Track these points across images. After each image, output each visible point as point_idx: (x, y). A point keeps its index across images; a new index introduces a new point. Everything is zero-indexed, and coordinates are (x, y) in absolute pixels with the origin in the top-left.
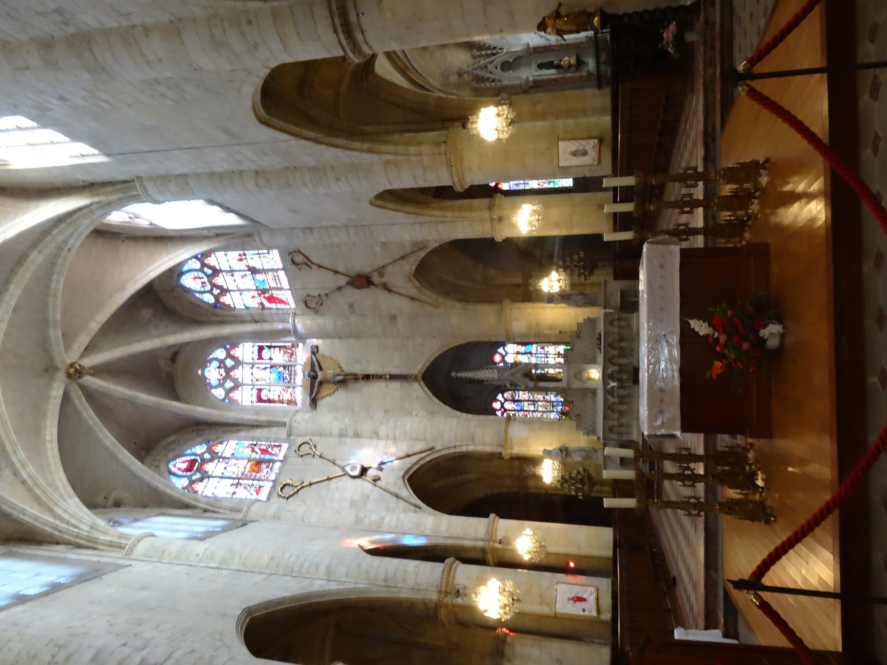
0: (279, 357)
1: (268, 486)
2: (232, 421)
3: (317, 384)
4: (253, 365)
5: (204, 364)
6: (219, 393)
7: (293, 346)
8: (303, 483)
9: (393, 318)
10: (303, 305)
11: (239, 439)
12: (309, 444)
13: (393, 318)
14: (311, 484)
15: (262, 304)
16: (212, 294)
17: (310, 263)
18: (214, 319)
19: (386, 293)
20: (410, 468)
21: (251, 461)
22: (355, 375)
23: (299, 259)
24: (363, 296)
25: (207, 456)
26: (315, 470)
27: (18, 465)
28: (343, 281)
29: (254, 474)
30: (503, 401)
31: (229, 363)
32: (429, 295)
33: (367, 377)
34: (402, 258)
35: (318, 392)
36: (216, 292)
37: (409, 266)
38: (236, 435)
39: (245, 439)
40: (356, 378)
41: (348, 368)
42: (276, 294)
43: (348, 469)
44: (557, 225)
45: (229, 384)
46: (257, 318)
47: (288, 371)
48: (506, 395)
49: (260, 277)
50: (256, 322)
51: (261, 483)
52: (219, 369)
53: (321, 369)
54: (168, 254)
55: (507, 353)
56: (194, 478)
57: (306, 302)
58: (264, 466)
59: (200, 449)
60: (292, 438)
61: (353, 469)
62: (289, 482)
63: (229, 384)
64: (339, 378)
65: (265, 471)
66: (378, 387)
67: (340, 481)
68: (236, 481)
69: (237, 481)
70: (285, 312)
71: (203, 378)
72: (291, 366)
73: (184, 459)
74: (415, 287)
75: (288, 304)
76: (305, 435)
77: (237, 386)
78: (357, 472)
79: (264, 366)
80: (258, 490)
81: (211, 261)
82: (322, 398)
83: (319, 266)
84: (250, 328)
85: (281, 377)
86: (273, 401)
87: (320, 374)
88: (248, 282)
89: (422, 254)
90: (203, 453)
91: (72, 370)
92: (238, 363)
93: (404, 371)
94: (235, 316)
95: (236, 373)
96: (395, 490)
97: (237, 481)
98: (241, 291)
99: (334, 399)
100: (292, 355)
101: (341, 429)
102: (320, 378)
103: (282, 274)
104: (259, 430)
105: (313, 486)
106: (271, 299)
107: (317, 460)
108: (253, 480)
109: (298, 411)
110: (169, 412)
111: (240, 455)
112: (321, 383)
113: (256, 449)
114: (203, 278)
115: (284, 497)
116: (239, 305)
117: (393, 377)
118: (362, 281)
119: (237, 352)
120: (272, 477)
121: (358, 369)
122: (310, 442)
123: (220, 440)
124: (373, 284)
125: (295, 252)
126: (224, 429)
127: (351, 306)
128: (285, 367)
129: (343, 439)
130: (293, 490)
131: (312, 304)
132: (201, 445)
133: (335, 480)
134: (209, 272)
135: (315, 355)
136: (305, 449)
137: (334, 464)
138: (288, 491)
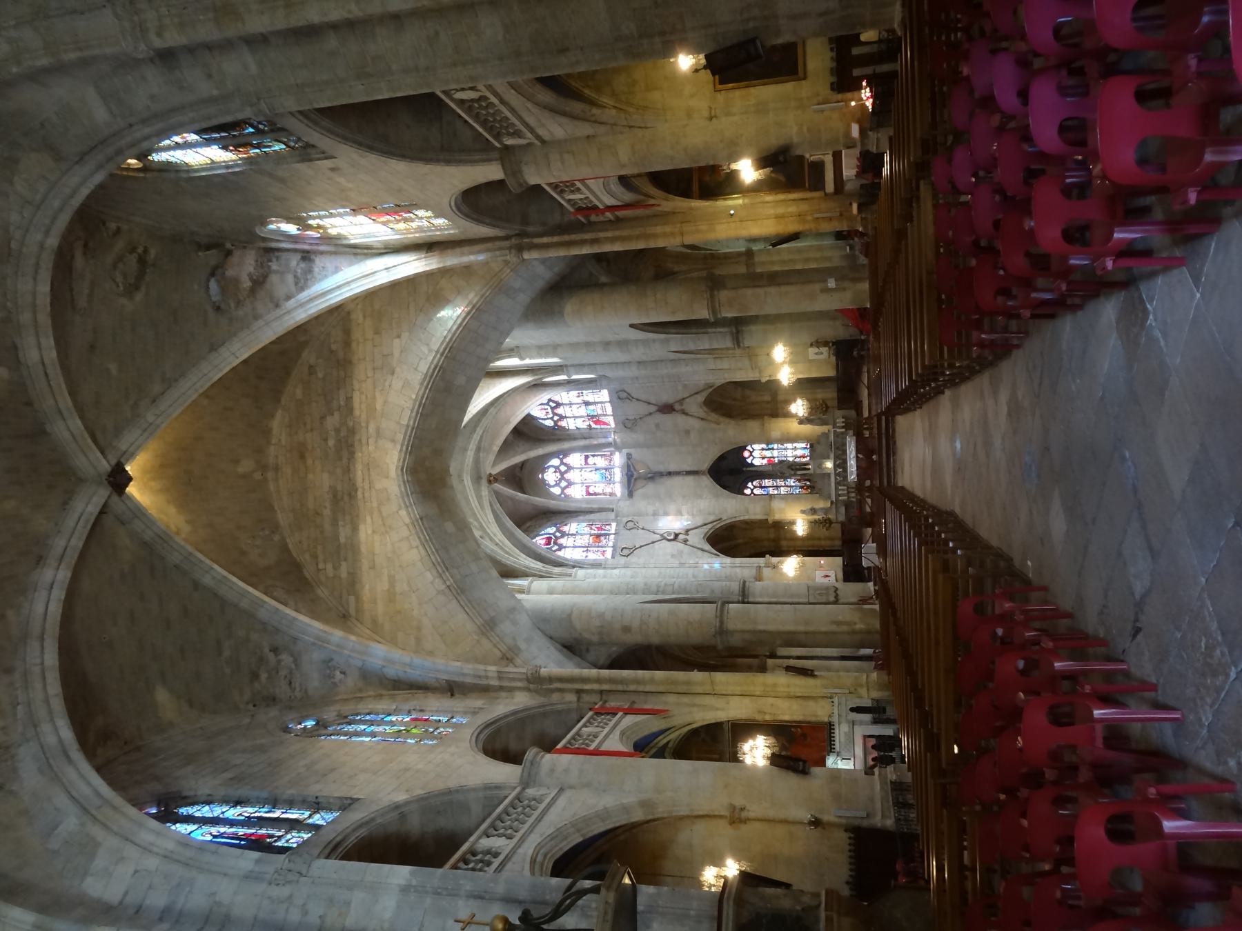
3: (633, 480)
4: (581, 469)
5: (543, 471)
6: (556, 491)
9: (687, 432)
10: (622, 426)
11: (579, 522)
13: (687, 432)
15: (590, 426)
18: (553, 437)
20: (708, 532)
22: (662, 473)
23: (624, 395)
24: (667, 420)
26: (641, 537)
27: (492, 535)
28: (653, 409)
29: (597, 544)
30: (752, 487)
32: (714, 416)
33: (670, 474)
34: (697, 393)
35: (634, 485)
37: (701, 398)
38: (576, 519)
39: (583, 521)
42: (603, 419)
43: (665, 535)
44: (801, 373)
45: (564, 484)
48: (754, 483)
49: (591, 407)
50: (585, 438)
51: (604, 549)
53: (635, 470)
54: (535, 397)
55: (754, 450)
58: (602, 538)
59: (551, 530)
62: (625, 546)
63: (564, 484)
64: (649, 475)
65: (604, 541)
66: (677, 480)
68: (585, 549)
69: (587, 548)
71: (543, 480)
74: (705, 412)
75: (610, 425)
77: (570, 484)
78: (672, 537)
79: (590, 469)
81: (557, 398)
82: (637, 489)
83: (638, 400)
84: (582, 443)
85: (603, 476)
86: (600, 494)
87: (635, 473)
88: (583, 411)
89: (711, 390)
90: (555, 532)
91: (492, 478)
92: (569, 468)
93: (695, 469)
94: (569, 435)
96: (700, 546)
97: (587, 548)
98: (575, 417)
99: (643, 490)
100: (611, 460)
102: (635, 477)
106: (597, 422)
107: (641, 531)
109: (619, 500)
110: (533, 505)
111: (583, 532)
112: (636, 479)
113: (593, 527)
116: (572, 427)
118: (667, 409)
120: (611, 544)
121: (661, 468)
124: (674, 410)
125: (621, 391)
126: (567, 515)
127: (657, 426)
128: (606, 469)
129: (656, 517)
134: (553, 405)
136: (630, 525)
138: (626, 552)
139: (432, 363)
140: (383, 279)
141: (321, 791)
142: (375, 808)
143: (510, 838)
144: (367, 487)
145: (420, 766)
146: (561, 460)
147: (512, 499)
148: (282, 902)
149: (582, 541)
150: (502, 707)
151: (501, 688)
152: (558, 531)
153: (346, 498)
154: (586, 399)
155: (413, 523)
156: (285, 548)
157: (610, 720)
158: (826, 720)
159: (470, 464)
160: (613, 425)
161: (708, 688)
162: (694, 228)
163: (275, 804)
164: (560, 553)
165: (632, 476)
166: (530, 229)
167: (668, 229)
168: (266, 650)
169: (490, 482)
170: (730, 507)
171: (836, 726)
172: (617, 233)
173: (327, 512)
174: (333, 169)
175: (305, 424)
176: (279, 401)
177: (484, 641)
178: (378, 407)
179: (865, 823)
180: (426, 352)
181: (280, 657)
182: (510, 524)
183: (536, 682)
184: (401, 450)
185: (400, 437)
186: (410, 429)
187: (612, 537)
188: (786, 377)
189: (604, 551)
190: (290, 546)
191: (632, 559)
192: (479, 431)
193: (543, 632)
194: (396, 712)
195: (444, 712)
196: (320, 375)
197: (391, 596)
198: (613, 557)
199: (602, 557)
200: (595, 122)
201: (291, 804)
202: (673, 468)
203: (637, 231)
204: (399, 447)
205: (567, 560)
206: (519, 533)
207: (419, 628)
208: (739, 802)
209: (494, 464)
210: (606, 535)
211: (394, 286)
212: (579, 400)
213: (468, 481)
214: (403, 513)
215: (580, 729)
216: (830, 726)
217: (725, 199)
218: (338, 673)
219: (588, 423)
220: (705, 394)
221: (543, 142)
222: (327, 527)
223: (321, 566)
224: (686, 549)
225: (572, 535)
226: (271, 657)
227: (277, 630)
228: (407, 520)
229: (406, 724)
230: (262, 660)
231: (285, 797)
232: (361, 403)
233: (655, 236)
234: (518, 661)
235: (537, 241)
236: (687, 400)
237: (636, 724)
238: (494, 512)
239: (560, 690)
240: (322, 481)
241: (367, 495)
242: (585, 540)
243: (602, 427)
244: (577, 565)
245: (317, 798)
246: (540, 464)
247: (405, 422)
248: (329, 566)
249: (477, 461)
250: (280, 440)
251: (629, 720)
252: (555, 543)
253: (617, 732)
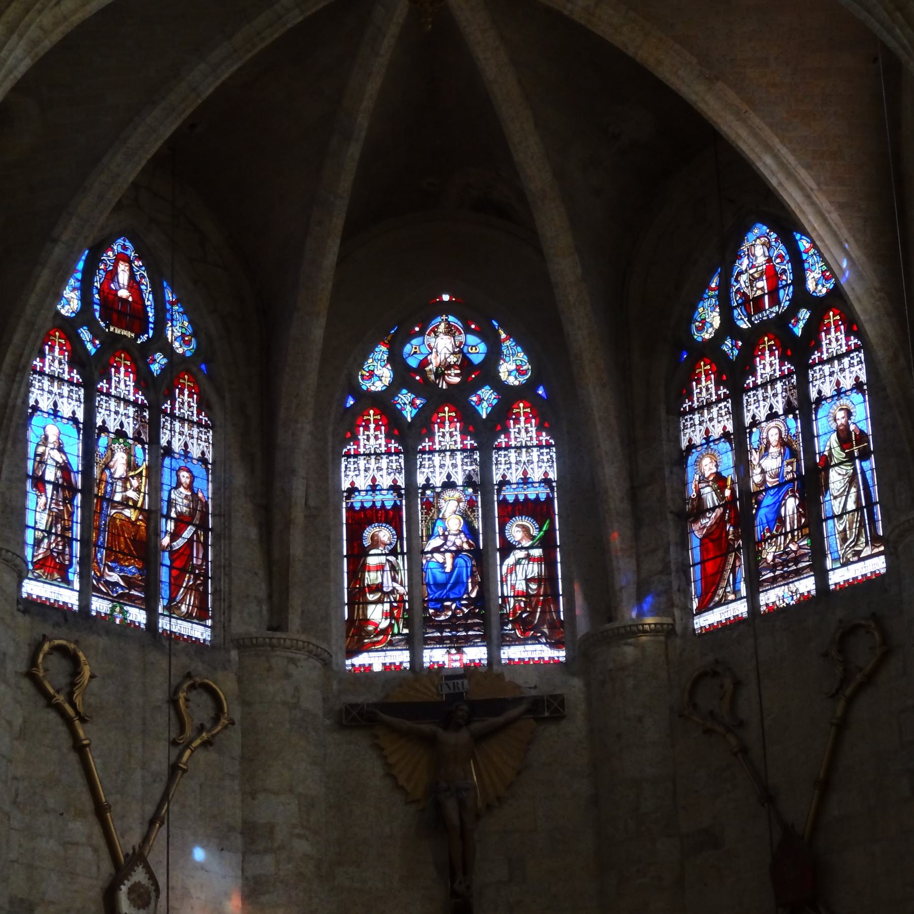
3: (426, 727)
7: (555, 626)
8: (83, 720)
12: (216, 720)
14: (80, 749)
15: (700, 510)
16: (720, 335)
17: (848, 691)
21: (147, 520)
25: (157, 366)
29: (104, 538)
43: (139, 876)
47: (466, 617)
50: (633, 495)
52: (460, 367)
53: (479, 738)
54: (840, 207)
56: (85, 334)
57: (715, 674)
60: (234, 654)
62: (87, 671)
64: (451, 807)
67: (96, 850)
68: (78, 480)
70: (677, 598)
72: (485, 625)
73: (146, 287)
76: (245, 703)
79: (479, 525)
82: (378, 748)
83: (842, 726)
87: (463, 736)
90: (168, 351)
101: (271, 829)
103: (807, 585)
104: (253, 533)
105: (73, 757)
107: (161, 757)
108: (85, 542)
109: (326, 663)
111: (167, 478)
113: (188, 533)
114: (775, 301)
115: (33, 662)
122: (224, 721)
123: (214, 398)
128: (482, 601)
129: (238, 841)
130: (58, 691)
132: (194, 334)
133: (97, 830)
135: (528, 711)
137: (152, 823)
146: (524, 392)
154: (837, 478)
160: (704, 621)
165: (448, 721)
189: (63, 571)
219: (710, 497)
225: (155, 429)
243: (695, 573)
252: (111, 345)
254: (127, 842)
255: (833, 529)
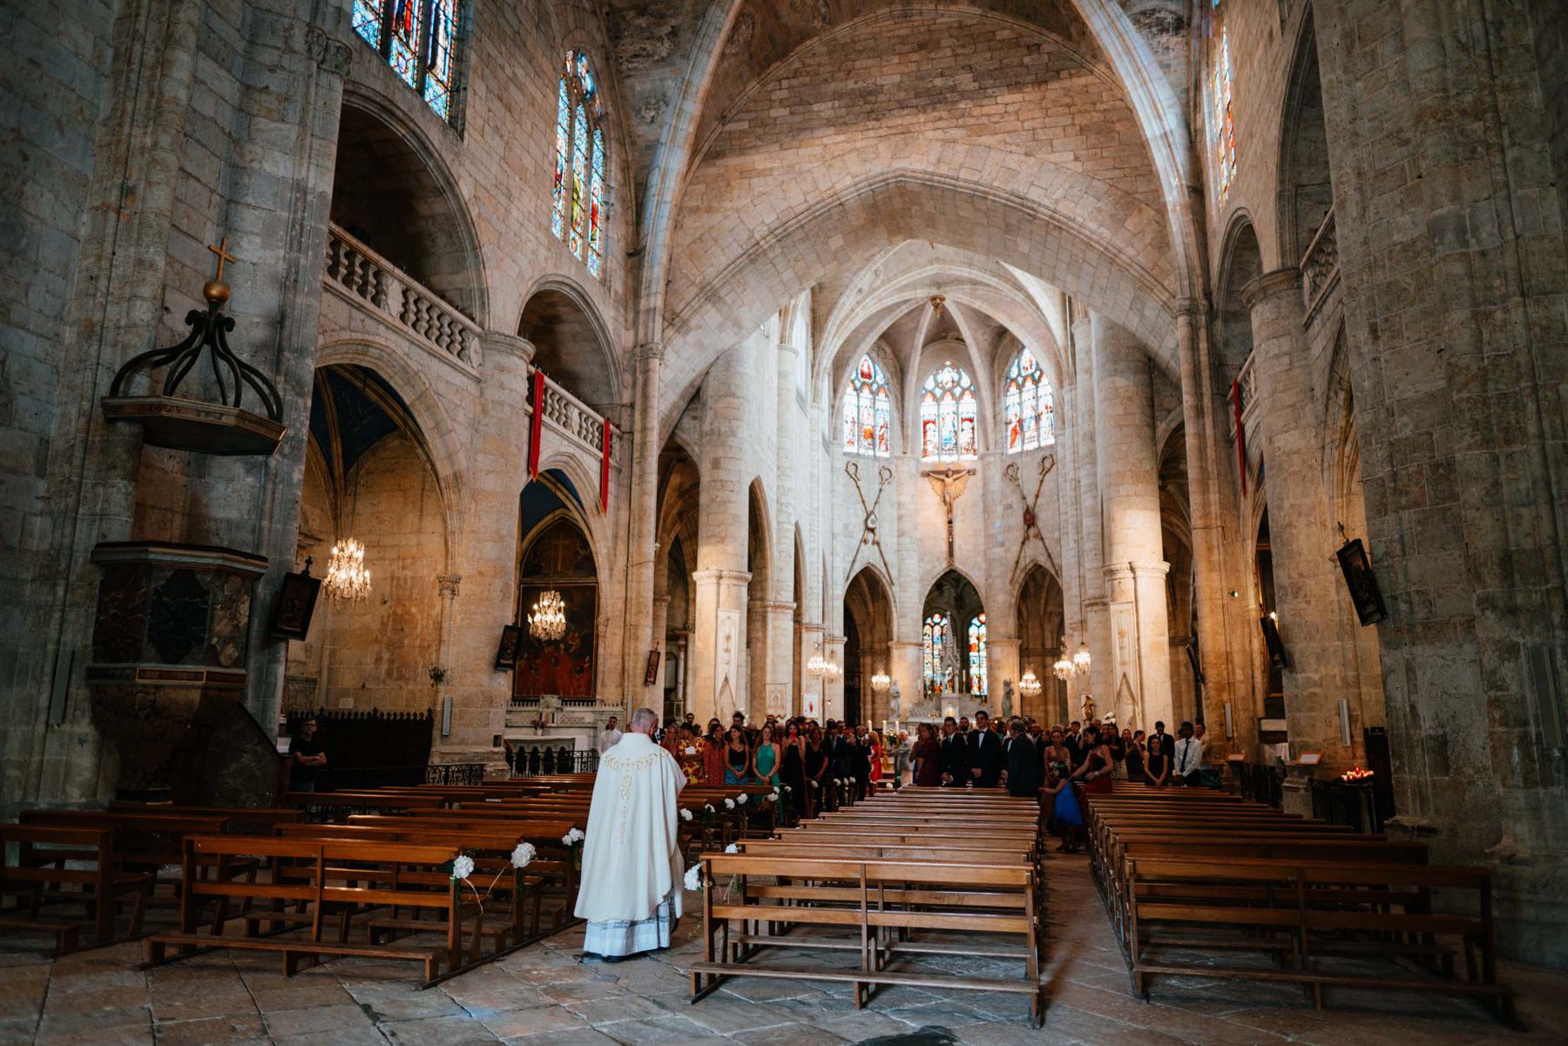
0: (965, 438)
1: (854, 449)
2: (906, 405)
6: (930, 384)
19: (1021, 540)
23: (1048, 464)
24: (1018, 519)
28: (1030, 501)
31: (958, 391)
32: (1020, 576)
34: (1049, 556)
36: (1020, 380)
37: (1043, 560)
39: (891, 418)
40: (950, 511)
41: (955, 504)
43: (873, 517)
46: (998, 418)
49: (1033, 423)
58: (870, 441)
59: (880, 379)
61: (873, 522)
63: (938, 392)
64: (947, 498)
65: (866, 443)
66: (944, 533)
69: (857, 422)
71: (943, 367)
78: (870, 525)
80: (851, 442)
81: (1044, 380)
84: (989, 414)
88: (1028, 413)
92: (957, 399)
93: (957, 553)
95: (948, 397)
96: (859, 558)
97: (857, 422)
98: (1020, 404)
102: (947, 480)
103: (1035, 445)
107: (878, 487)
117: (951, 545)
118: (1030, 519)
119: (967, 397)
120: (862, 451)
121: (957, 511)
124: (1029, 527)
127: (1010, 507)
131: (1010, 471)
134: (1037, 375)
136: (886, 475)
138: (852, 469)
139: (1039, 204)
140: (1151, 129)
141: (475, 93)
142: (448, 158)
143: (403, 317)
144: (881, 132)
145: (515, 213)
146: (968, 388)
147: (916, 328)
148: (286, 42)
149: (866, 416)
150: (608, 314)
151: (637, 313)
152: (880, 388)
153: (868, 107)
154: (1044, 417)
155: (835, 194)
156: (805, 36)
157: (591, 442)
158: (598, 697)
159: (952, 272)
160: (1010, 451)
161: (635, 559)
162: (1215, 543)
163: (460, 39)
164: (850, 390)
166: (1219, 324)
167: (1215, 509)
168: (673, 22)
169: (934, 299)
170: (908, 597)
171: (590, 709)
172: (1210, 442)
173: (851, 84)
174: (1271, 34)
175: (963, 46)
176: (992, 9)
177: (694, 290)
178: (983, 139)
179: (436, 733)
180: (1055, 197)
181: (666, 40)
182: (884, 326)
183: (643, 354)
184: (926, 173)
185: (944, 170)
186: (953, 182)
187: (871, 453)
188: (1063, 666)
190: (808, 43)
191: (843, 477)
192: (994, 281)
193: (712, 365)
194: (607, 188)
195: (606, 247)
196: (1027, 60)
197: (746, 174)
198: (845, 454)
199: (845, 440)
200: (1328, 398)
201: (458, 59)
202: (957, 526)
203: (1212, 468)
204: (930, 169)
205: (842, 398)
206: (874, 337)
207: (709, 210)
208: (463, 588)
209: (958, 304)
210: (874, 445)
211: (1142, 146)
212: (1042, 409)
213: (932, 270)
214: (848, 181)
215: (575, 406)
216: (590, 701)
217: (1256, 585)
218: (653, 113)
220: (1048, 566)
221: (1307, 326)
222: (832, 86)
223: (785, 83)
224: (855, 542)
226: (666, 29)
227: (696, 33)
228: (838, 187)
229: (587, 200)
230: (661, 17)
231: (467, 51)
232: (989, 116)
233: (1205, 491)
234: (670, 332)
235: (1203, 334)
236: (1041, 544)
237: (586, 474)
238: (898, 305)
239: (634, 385)
240: (890, 75)
241: (871, 133)
242: (868, 422)
244: (835, 409)
245: (465, 89)
246: (962, 361)
247: (963, 175)
248: (784, 94)
249: (958, 281)
250: (943, 15)
251: (593, 466)
252: (864, 384)
253: (572, 450)
254: (870, 509)
255: (1042, 431)
